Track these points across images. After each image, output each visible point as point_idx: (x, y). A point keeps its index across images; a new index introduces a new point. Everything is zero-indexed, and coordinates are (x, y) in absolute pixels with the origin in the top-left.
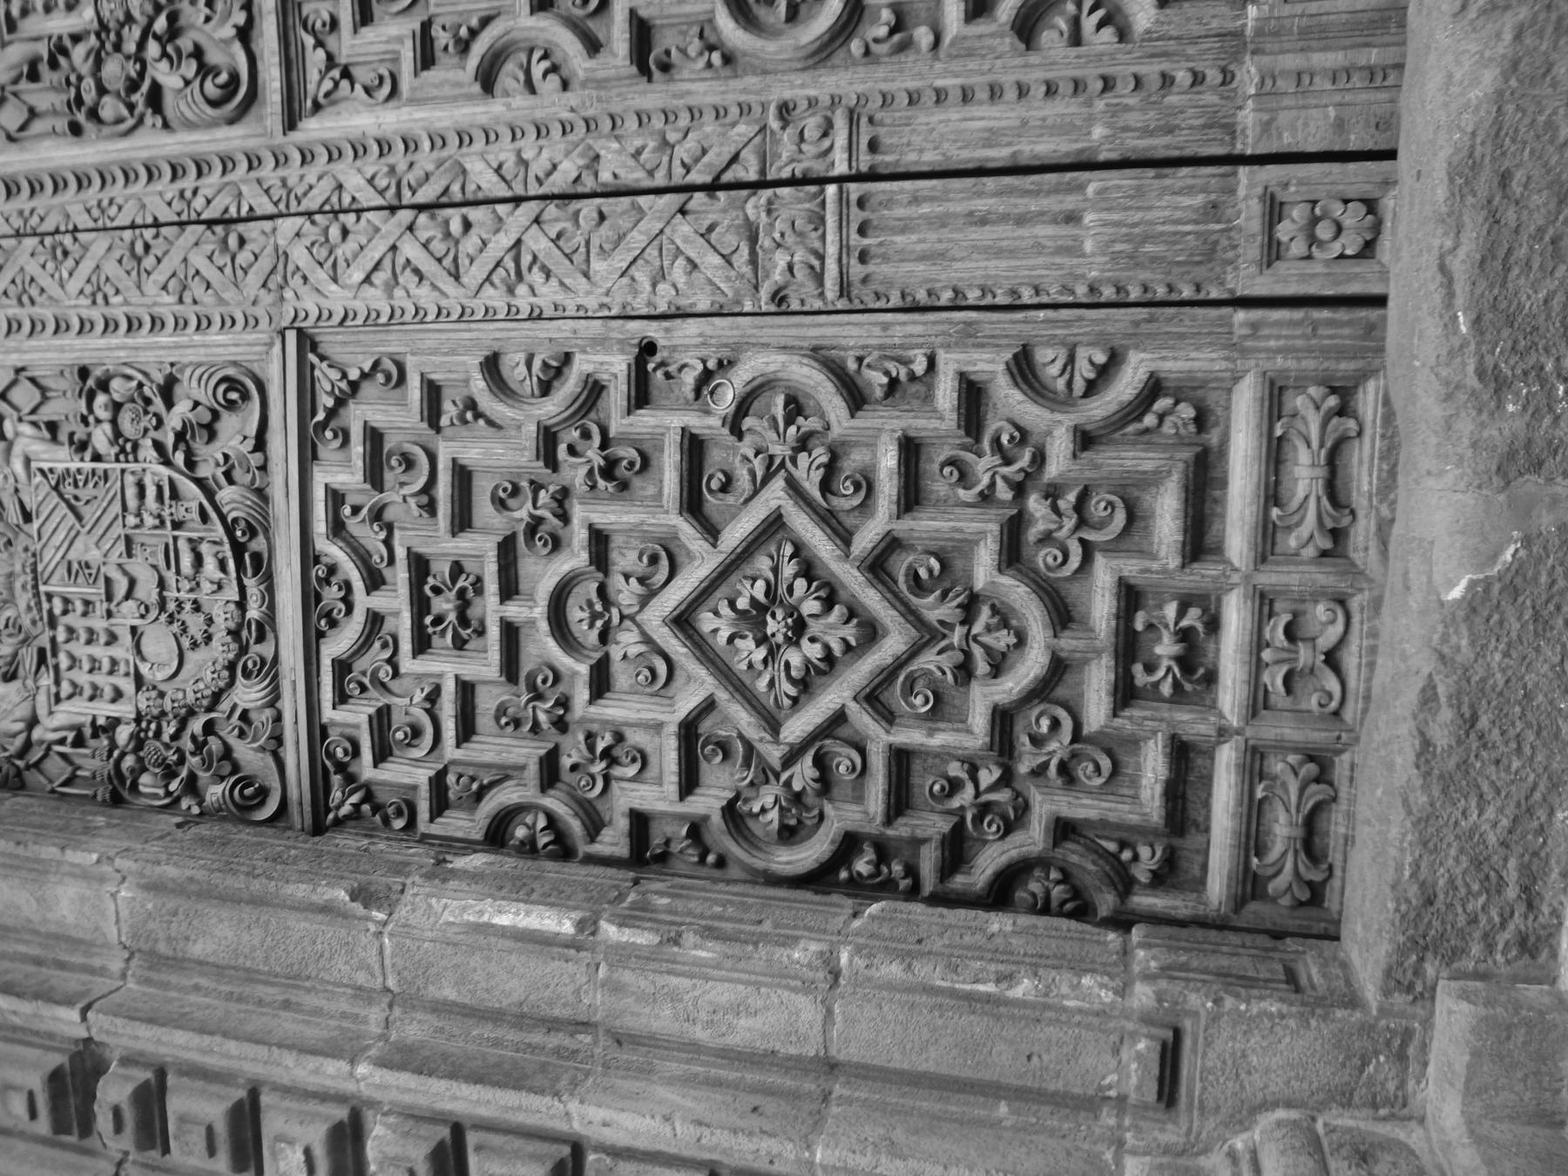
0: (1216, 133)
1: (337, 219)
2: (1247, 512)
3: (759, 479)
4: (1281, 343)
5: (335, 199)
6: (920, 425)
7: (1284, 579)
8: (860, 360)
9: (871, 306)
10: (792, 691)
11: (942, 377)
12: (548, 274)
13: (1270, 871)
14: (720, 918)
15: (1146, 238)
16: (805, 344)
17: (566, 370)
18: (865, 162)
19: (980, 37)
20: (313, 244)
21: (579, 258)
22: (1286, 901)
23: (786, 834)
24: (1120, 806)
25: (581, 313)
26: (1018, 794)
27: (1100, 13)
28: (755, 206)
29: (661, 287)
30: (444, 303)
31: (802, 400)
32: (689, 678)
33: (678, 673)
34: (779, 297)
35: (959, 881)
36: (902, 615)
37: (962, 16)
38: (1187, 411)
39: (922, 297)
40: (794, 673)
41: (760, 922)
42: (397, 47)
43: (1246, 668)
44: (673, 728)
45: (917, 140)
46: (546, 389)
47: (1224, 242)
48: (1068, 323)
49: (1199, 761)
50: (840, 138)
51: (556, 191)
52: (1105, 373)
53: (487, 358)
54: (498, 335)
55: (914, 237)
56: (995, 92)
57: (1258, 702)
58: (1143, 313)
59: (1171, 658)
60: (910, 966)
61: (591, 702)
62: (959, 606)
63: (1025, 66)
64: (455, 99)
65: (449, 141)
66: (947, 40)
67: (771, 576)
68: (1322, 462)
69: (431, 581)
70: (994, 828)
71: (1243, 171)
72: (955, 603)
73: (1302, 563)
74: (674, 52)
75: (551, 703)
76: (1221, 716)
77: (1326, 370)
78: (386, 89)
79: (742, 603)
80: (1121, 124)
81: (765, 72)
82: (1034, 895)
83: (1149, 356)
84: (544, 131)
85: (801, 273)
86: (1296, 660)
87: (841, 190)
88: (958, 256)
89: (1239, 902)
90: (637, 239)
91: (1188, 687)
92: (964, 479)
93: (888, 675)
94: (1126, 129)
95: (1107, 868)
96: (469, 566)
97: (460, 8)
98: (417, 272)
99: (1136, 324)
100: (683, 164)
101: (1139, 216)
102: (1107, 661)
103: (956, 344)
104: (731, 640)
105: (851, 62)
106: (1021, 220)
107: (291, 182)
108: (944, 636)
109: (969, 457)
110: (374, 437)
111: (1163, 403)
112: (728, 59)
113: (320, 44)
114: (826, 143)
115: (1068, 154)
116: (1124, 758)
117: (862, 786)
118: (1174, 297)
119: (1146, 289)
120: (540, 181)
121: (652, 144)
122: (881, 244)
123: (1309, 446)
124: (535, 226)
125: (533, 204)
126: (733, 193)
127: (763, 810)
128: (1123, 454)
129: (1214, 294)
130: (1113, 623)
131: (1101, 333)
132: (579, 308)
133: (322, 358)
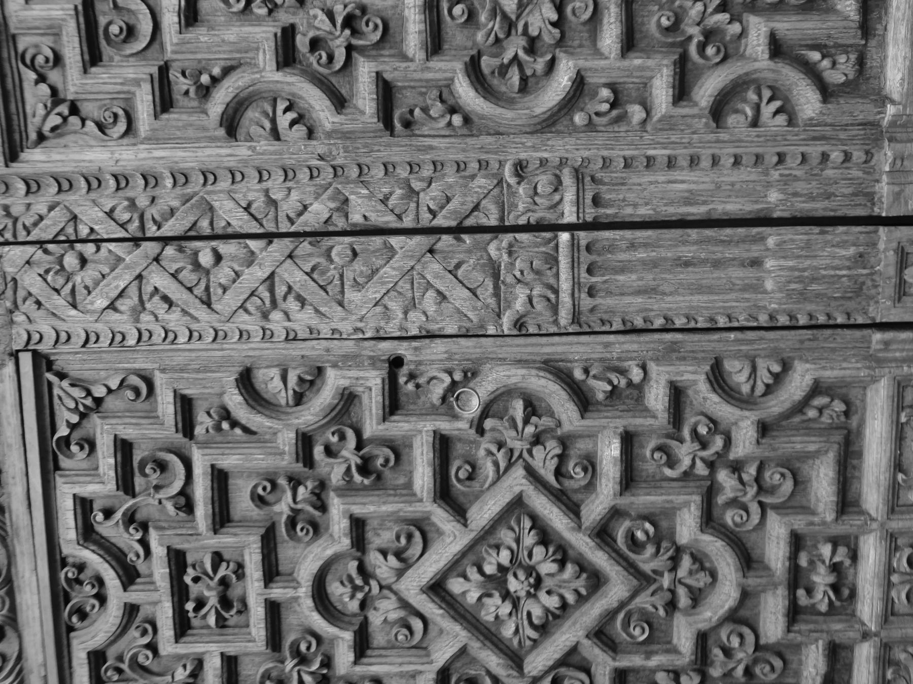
0: (861, 200)
1: (73, 248)
2: (882, 477)
3: (502, 469)
4: (904, 354)
5: (70, 230)
6: (637, 422)
8: (586, 371)
9: (597, 329)
10: (533, 634)
11: (652, 383)
12: (302, 301)
15: (814, 280)
16: (538, 358)
17: (318, 382)
18: (590, 214)
19: (683, 117)
20: (47, 271)
21: (333, 289)
25: (337, 336)
27: (777, 104)
28: (496, 248)
29: (412, 315)
30: (194, 326)
31: (536, 403)
32: (441, 631)
33: (431, 627)
34: (519, 324)
37: (670, 99)
38: (839, 406)
39: (639, 323)
40: (536, 621)
42: (133, 89)
45: (631, 196)
46: (299, 399)
47: (869, 283)
48: (750, 342)
49: (843, 654)
50: (569, 195)
51: (308, 229)
54: (251, 353)
55: (634, 277)
56: (694, 161)
57: (889, 613)
61: (355, 663)
63: (718, 141)
64: (198, 140)
65: (192, 179)
66: (657, 115)
67: (514, 546)
69: (190, 570)
71: (882, 231)
72: (666, 557)
74: (417, 112)
76: (863, 624)
78: (122, 126)
79: (490, 569)
80: (790, 190)
81: (499, 133)
83: (813, 366)
84: (291, 174)
85: (539, 306)
87: (573, 236)
88: (667, 290)
90: (389, 272)
92: (672, 462)
93: (611, 615)
94: (795, 194)
97: (199, 56)
98: (166, 299)
99: (802, 342)
100: (430, 211)
101: (808, 263)
102: (782, 592)
104: (480, 599)
105: (574, 130)
106: (717, 264)
107: (15, 211)
108: (655, 580)
109: (673, 443)
110: (124, 448)
112: (467, 120)
113: (42, 79)
114: (557, 197)
115: (751, 212)
116: (789, 657)
118: (831, 322)
119: (811, 316)
120: (291, 221)
121: (399, 192)
122: (605, 282)
124: (289, 261)
125: (287, 241)
126: (478, 236)
129: (860, 320)
130: (787, 564)
131: (775, 348)
133: (62, 376)
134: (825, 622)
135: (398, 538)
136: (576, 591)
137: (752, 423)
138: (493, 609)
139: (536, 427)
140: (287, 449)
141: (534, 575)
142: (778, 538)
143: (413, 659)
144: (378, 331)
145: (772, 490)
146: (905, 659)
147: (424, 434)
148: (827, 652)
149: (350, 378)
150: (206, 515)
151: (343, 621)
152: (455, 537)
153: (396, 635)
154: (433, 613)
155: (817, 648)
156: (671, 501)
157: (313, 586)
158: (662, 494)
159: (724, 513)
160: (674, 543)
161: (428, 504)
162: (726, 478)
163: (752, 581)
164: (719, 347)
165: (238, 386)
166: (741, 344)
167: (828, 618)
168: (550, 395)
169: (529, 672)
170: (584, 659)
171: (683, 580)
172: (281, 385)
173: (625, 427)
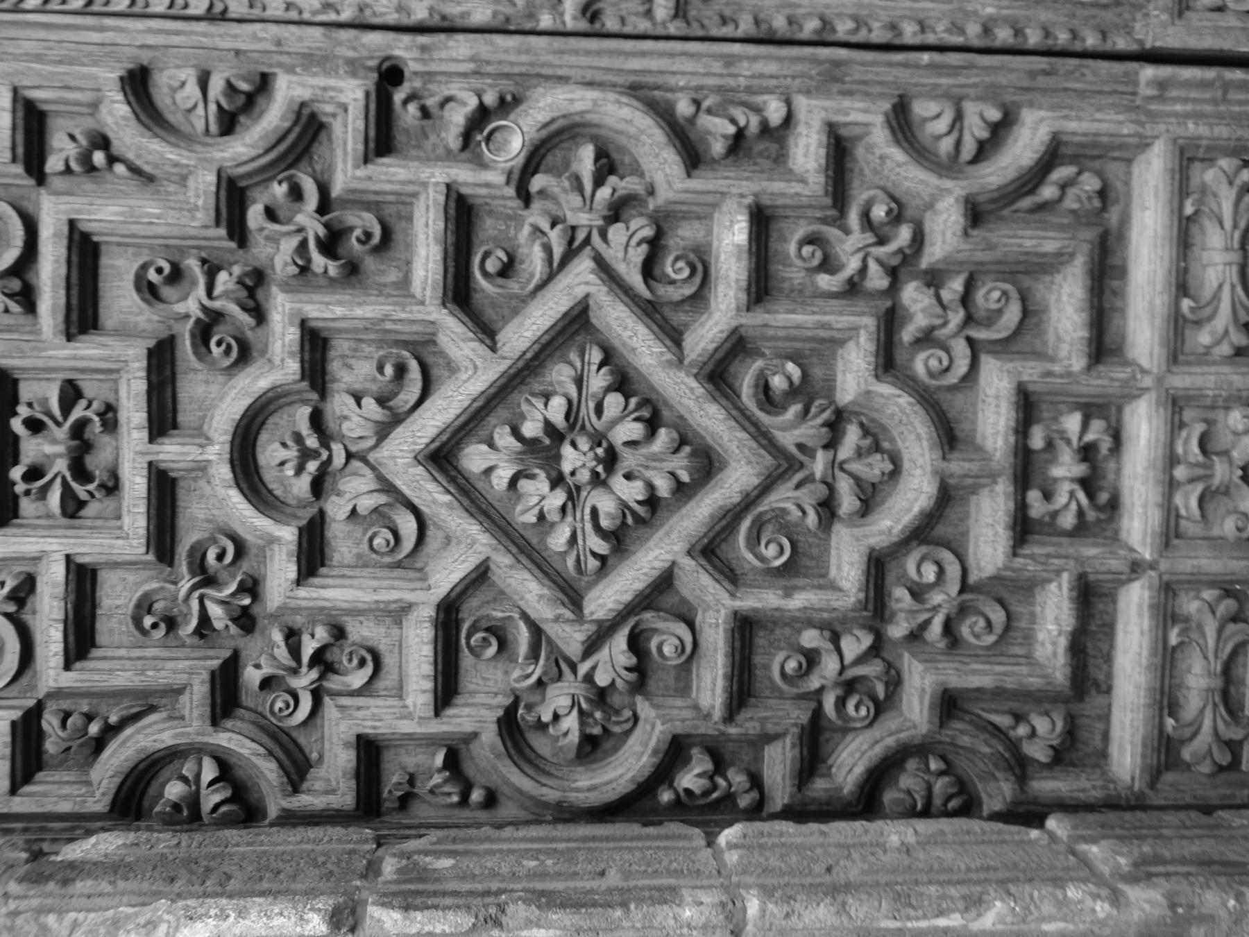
2: (1158, 301)
4: (1189, 107)
6: (775, 188)
7: (1199, 381)
8: (697, 103)
9: (715, 32)
10: (601, 546)
11: (802, 129)
13: (1188, 732)
14: (543, 875)
16: (620, 80)
17: (261, 100)
22: (1206, 768)
23: (588, 748)
24: (1016, 669)
25: (293, 15)
26: (889, 666)
31: (615, 155)
32: (448, 540)
33: (431, 532)
35: (819, 786)
36: (754, 437)
38: (1090, 183)
40: (605, 523)
41: (602, 874)
43: (1160, 489)
44: (428, 612)
46: (228, 124)
49: (1101, 606)
52: (999, 131)
53: (131, 73)
54: (151, 40)
58: (1042, 63)
59: (1073, 480)
60: (844, 904)
61: (299, 582)
62: (823, 425)
67: (573, 391)
68: (1236, 245)
69: (23, 411)
70: (863, 711)
72: (819, 421)
73: (1214, 363)
75: (233, 587)
76: (1132, 550)
77: (1238, 140)
79: (531, 429)
82: (909, 792)
83: (1050, 114)
86: (1210, 476)
89: (1154, 775)
91: (1091, 515)
92: (828, 265)
93: (729, 519)
95: (1001, 749)
96: (89, 388)
99: (1033, 74)
103: (818, 89)
108: (802, 466)
109: (832, 232)
111: (1063, 172)
116: (1016, 608)
117: (689, 671)
118: (1078, 46)
119: (1047, 34)
123: (1222, 227)
127: (556, 717)
128: (1020, 233)
130: (1012, 439)
132: (289, 7)
134: (1072, 544)
135: (380, 369)
136: (672, 474)
137: (957, 200)
138: (535, 500)
139: (614, 190)
140: (200, 203)
141: (605, 444)
142: (997, 397)
143: (397, 583)
144: (361, 10)
145: (991, 319)
146: (1199, 610)
147: (431, 190)
148: (1075, 594)
149: (312, 87)
150: (54, 307)
151: (282, 512)
152: (476, 367)
153: (371, 540)
154: (435, 502)
155: (1060, 587)
156: (826, 326)
157: (232, 442)
158: (814, 313)
159: (912, 360)
160: (832, 402)
161: (433, 308)
162: (915, 295)
163: (957, 466)
164: (904, 76)
165: (123, 89)
166: (941, 75)
167: (1076, 540)
168: (636, 138)
169: (592, 613)
170: (684, 601)
171: (845, 466)
172: (197, 93)
173: (755, 195)
